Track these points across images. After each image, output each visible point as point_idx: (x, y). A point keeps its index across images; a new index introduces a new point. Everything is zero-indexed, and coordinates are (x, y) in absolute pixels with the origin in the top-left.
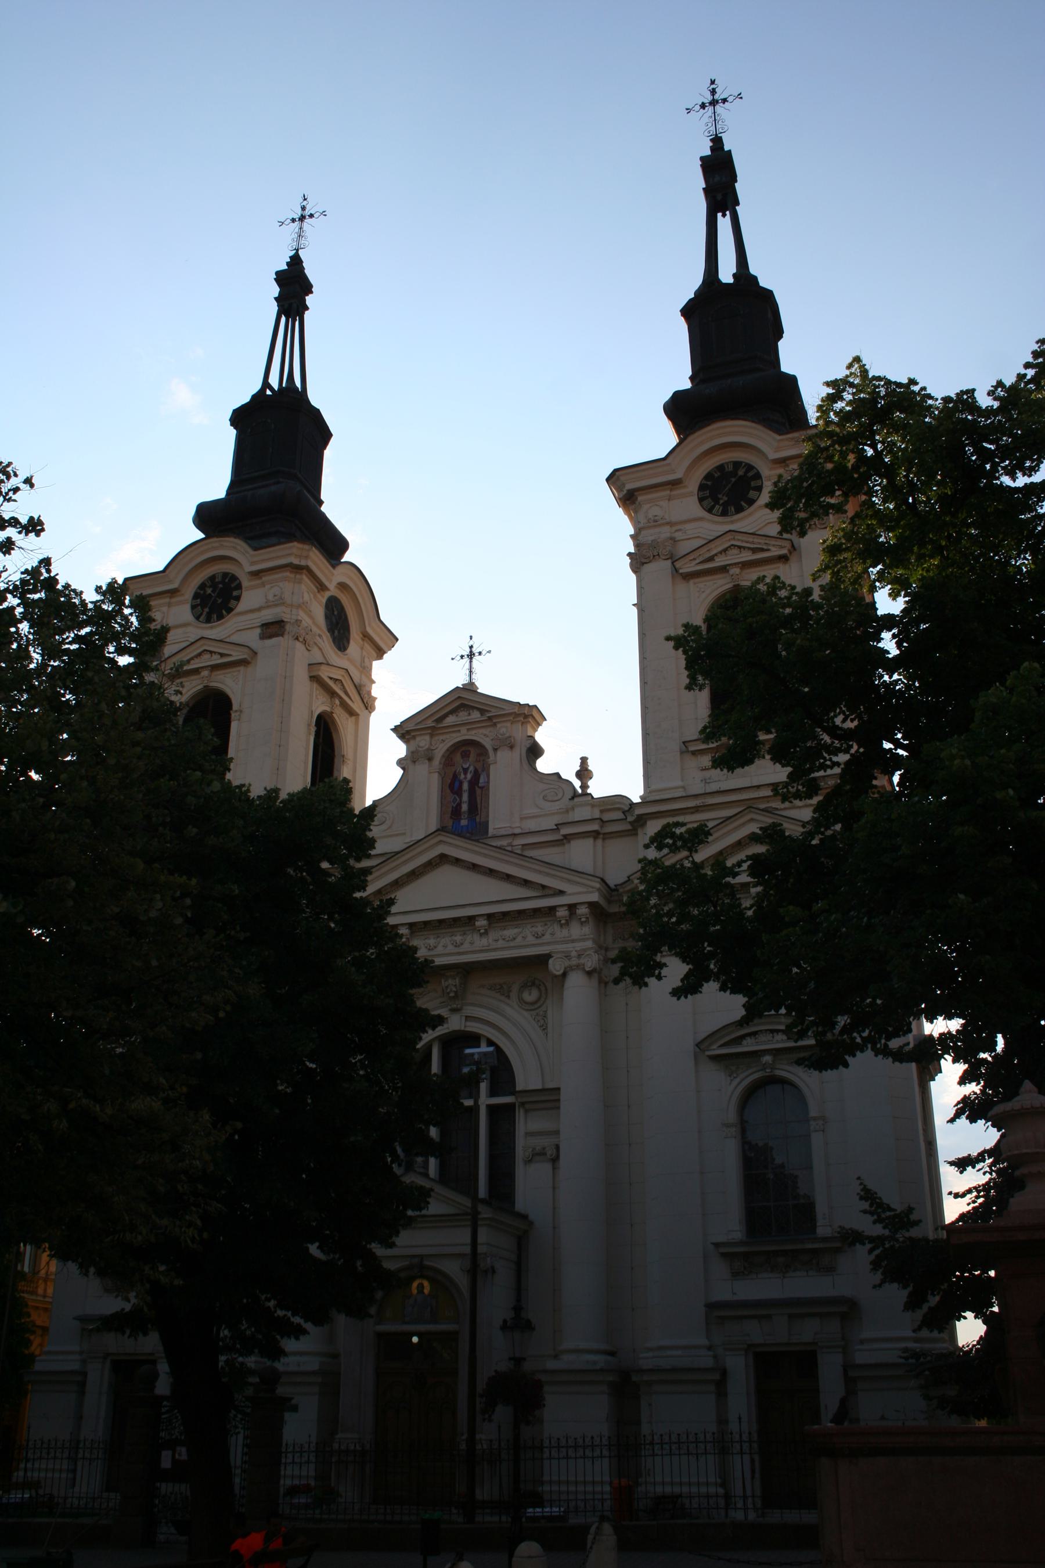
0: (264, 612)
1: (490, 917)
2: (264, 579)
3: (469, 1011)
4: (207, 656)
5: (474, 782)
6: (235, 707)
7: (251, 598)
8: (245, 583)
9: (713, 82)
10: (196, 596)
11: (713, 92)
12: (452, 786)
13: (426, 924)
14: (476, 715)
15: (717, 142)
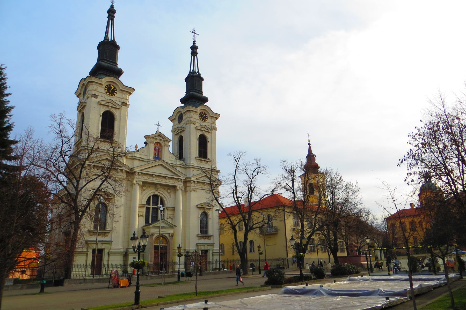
1: (169, 177)
3: (159, 191)
5: (159, 150)
6: (116, 117)
7: (118, 94)
10: (106, 87)
12: (155, 149)
13: (158, 176)
14: (162, 139)
15: (194, 42)
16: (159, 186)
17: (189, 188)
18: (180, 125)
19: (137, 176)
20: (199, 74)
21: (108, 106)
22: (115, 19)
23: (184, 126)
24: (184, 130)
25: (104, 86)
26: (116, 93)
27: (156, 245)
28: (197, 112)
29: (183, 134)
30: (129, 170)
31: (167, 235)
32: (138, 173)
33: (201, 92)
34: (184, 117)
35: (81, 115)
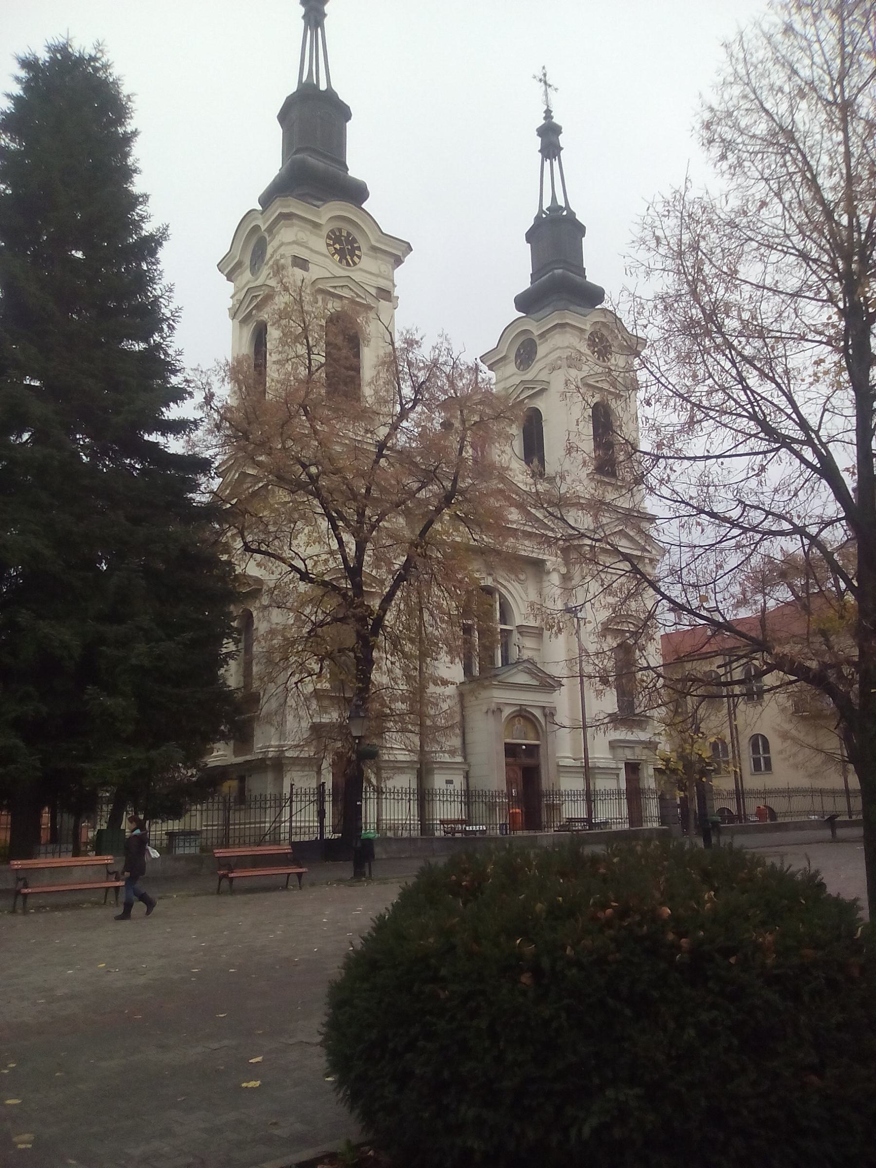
0: (380, 279)
2: (378, 255)
4: (347, 291)
7: (367, 263)
8: (364, 249)
9: (544, 68)
10: (329, 237)
11: (545, 75)
15: (548, 113)
18: (528, 376)
20: (572, 214)
22: (326, 21)
23: (543, 376)
24: (543, 391)
25: (325, 232)
26: (359, 257)
27: (508, 741)
28: (582, 331)
29: (540, 404)
31: (538, 713)
33: (581, 271)
34: (542, 350)
35: (248, 332)
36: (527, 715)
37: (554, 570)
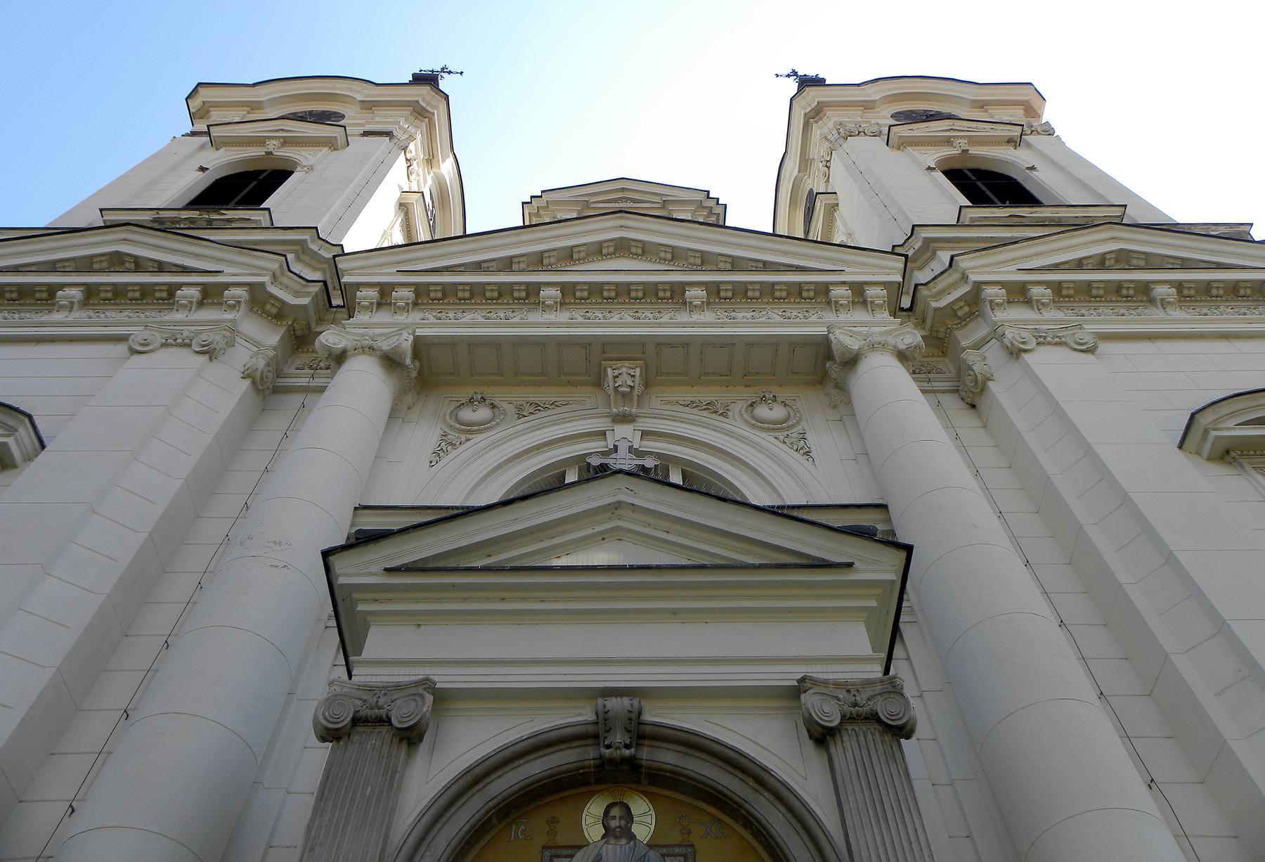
16: (626, 375)
17: (993, 351)
19: (383, 316)
21: (261, 141)
30: (305, 301)
32: (385, 290)
36: (668, 757)
37: (872, 347)
